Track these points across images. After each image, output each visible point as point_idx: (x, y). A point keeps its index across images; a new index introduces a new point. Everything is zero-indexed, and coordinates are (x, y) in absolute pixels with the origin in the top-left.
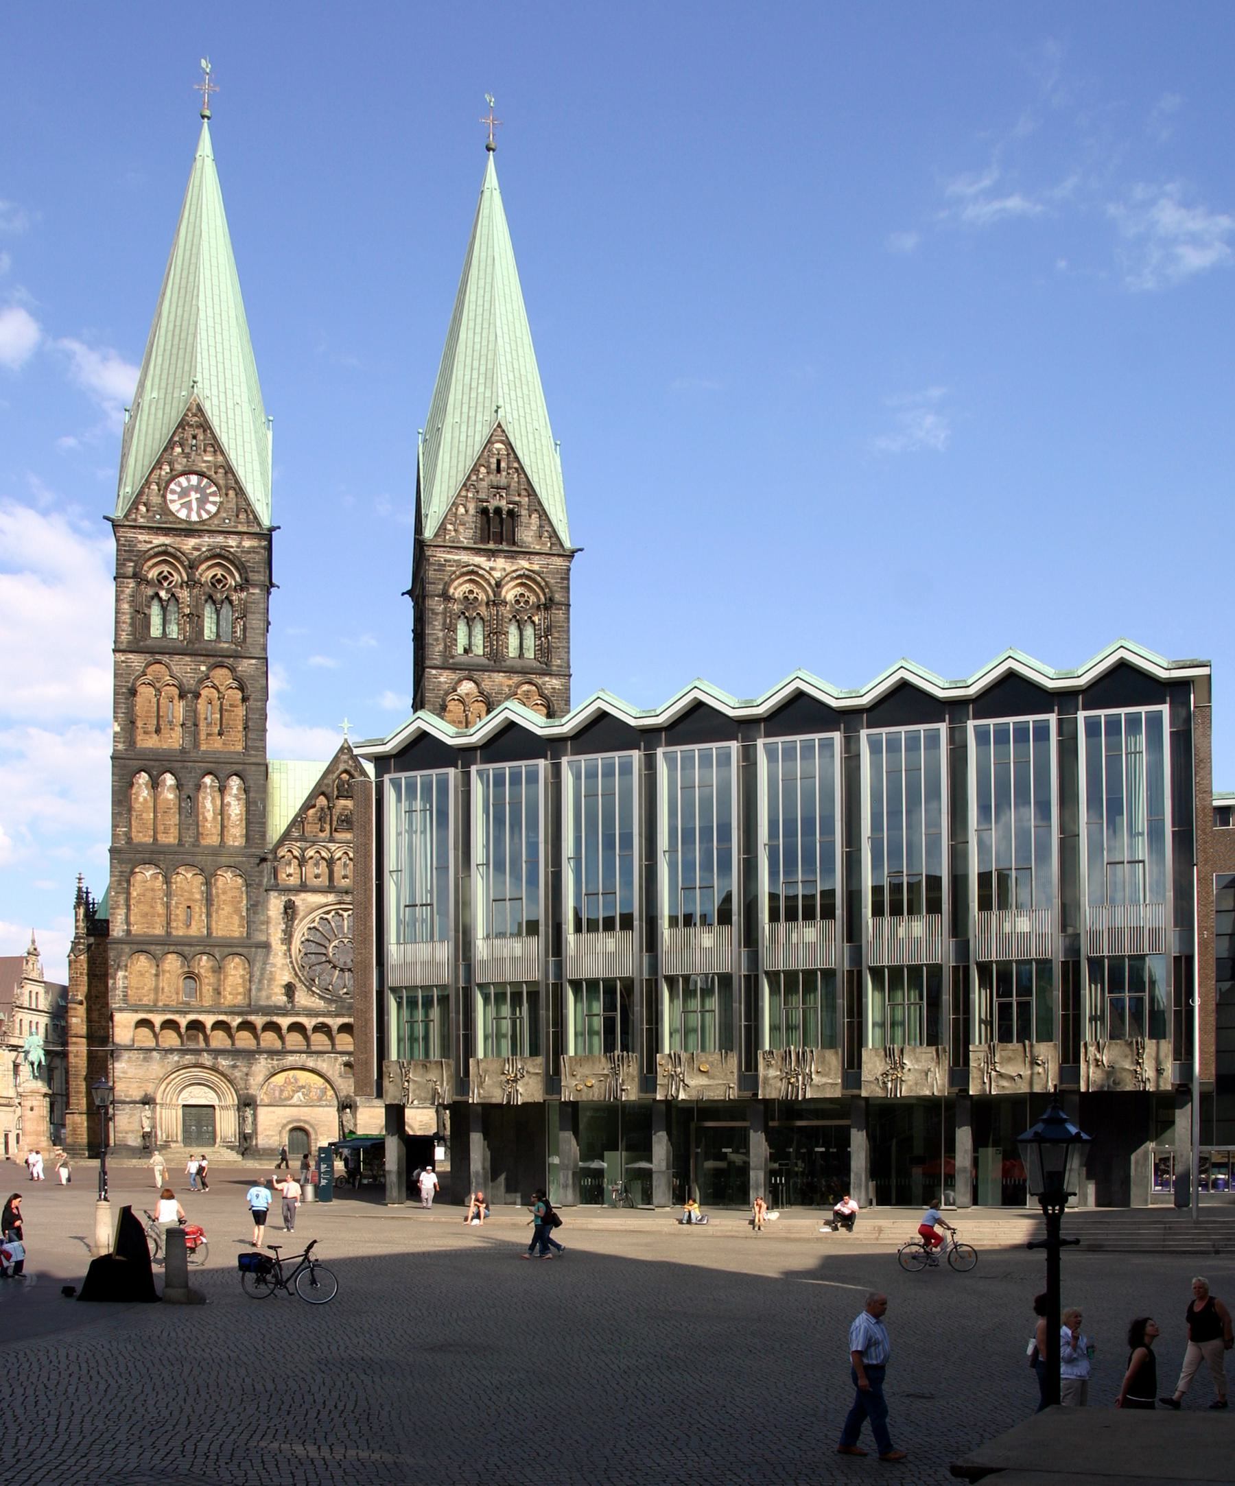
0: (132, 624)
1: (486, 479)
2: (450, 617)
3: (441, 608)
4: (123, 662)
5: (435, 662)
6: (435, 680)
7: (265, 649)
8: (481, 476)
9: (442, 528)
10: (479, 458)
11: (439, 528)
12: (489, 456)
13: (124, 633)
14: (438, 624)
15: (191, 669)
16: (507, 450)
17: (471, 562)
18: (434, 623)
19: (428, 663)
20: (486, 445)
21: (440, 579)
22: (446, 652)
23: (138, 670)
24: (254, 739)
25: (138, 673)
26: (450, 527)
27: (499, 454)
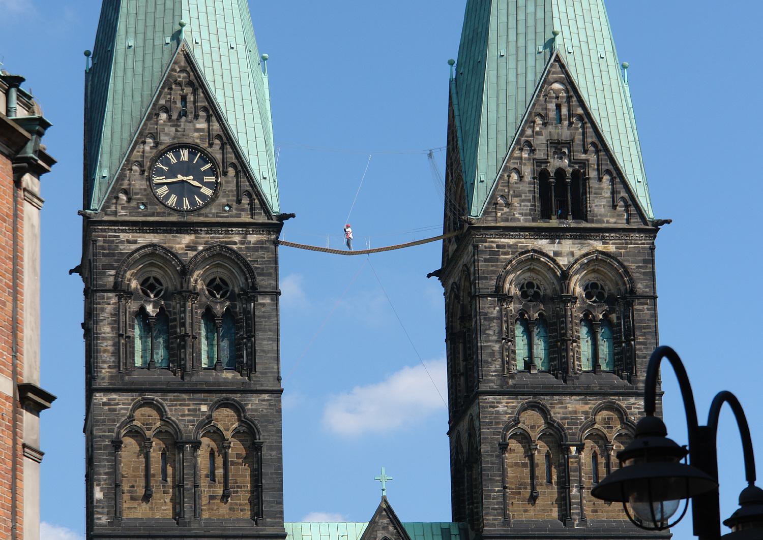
0: (116, 353)
1: (544, 132)
2: (507, 322)
3: (495, 312)
4: (104, 404)
5: (492, 384)
6: (491, 409)
7: (279, 379)
8: (537, 129)
9: (493, 203)
10: (534, 105)
11: (489, 203)
12: (546, 101)
13: (106, 366)
14: (492, 332)
15: (189, 410)
16: (567, 91)
17: (530, 247)
18: (488, 332)
19: (483, 387)
20: (542, 87)
21: (494, 272)
22: (503, 370)
23: (123, 415)
24: (269, 502)
25: (123, 419)
26: (500, 201)
27: (557, 98)
